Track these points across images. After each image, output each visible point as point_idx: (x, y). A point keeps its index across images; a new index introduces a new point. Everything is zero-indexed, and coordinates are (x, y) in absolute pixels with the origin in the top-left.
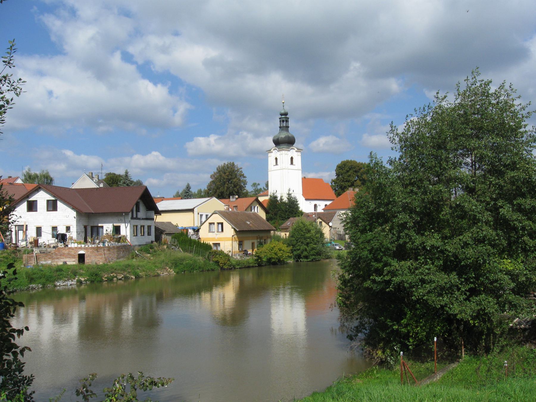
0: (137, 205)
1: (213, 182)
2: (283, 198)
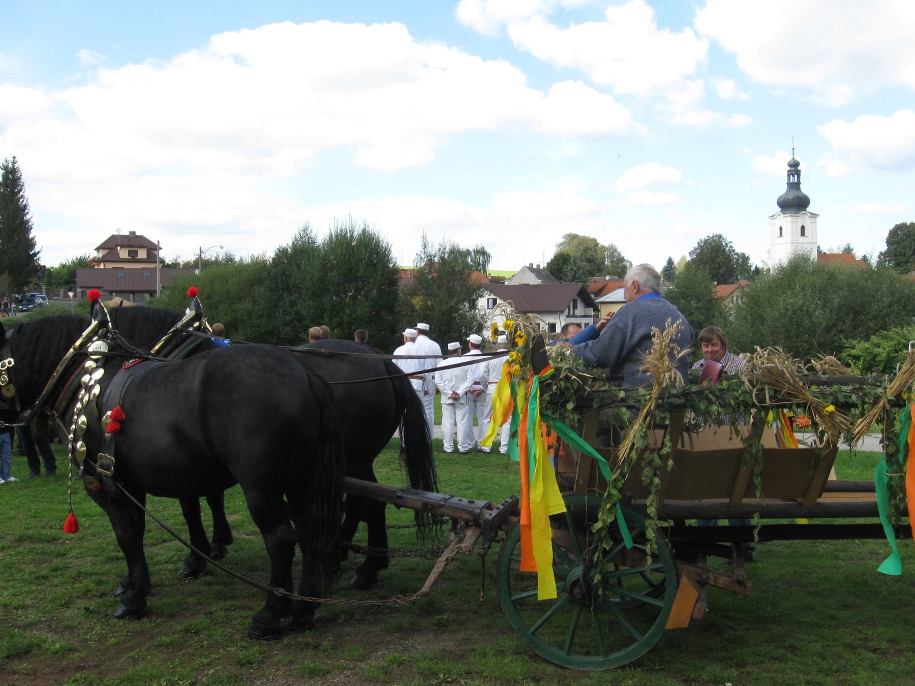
0: (575, 302)
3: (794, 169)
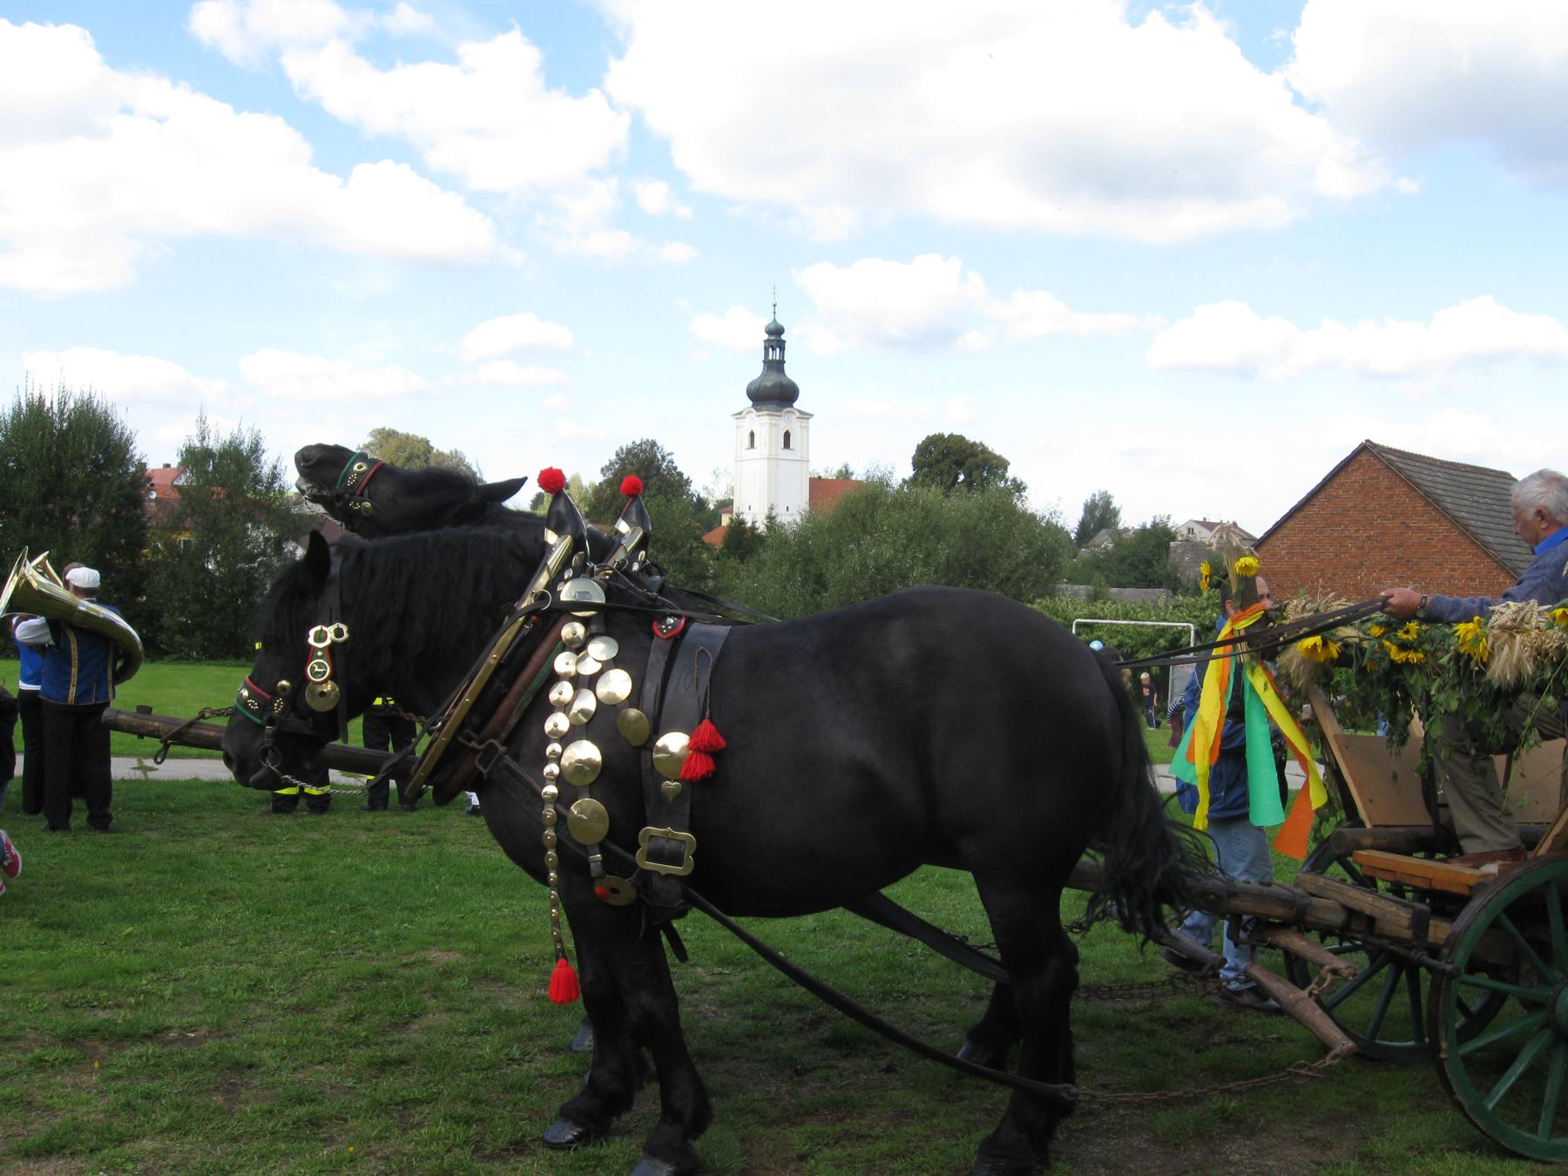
1: (608, 483)
2: (757, 525)
3: (775, 338)
